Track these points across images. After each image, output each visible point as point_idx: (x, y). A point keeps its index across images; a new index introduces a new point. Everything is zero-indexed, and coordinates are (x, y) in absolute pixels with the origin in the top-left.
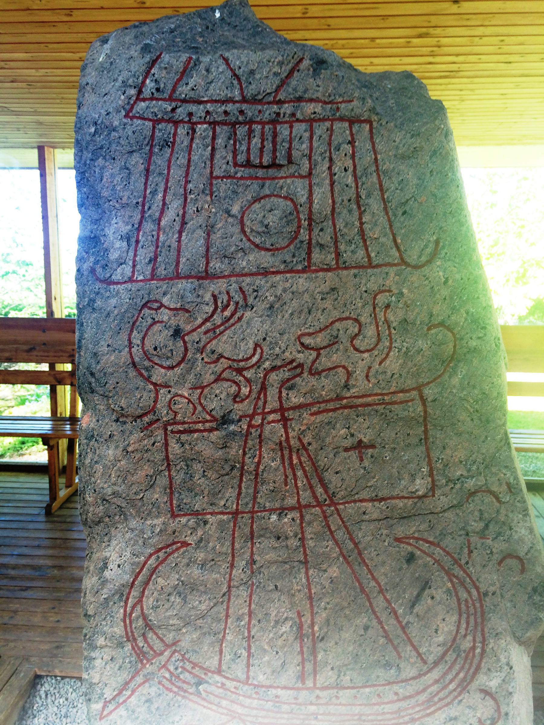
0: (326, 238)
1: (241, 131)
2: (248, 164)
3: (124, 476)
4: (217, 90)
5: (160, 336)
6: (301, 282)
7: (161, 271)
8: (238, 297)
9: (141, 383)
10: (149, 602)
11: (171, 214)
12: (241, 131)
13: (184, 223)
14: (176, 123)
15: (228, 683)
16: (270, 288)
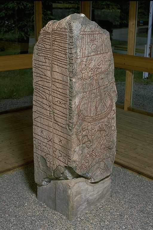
0: (99, 50)
1: (91, 36)
2: (91, 40)
3: (79, 87)
4: (89, 30)
5: (84, 66)
6: (97, 56)
7: (83, 56)
8: (91, 59)
9: (81, 73)
10: (80, 107)
11: (84, 48)
12: (91, 36)
13: (85, 49)
14: (84, 35)
15: (88, 118)
16: (94, 57)
